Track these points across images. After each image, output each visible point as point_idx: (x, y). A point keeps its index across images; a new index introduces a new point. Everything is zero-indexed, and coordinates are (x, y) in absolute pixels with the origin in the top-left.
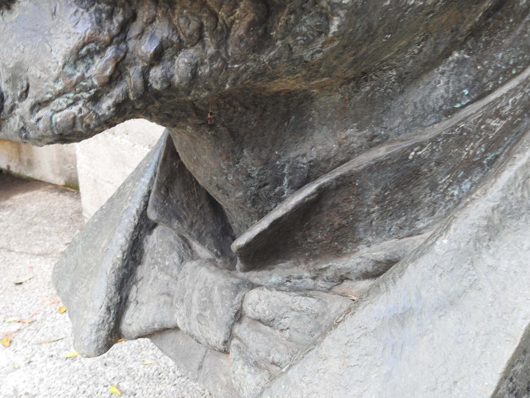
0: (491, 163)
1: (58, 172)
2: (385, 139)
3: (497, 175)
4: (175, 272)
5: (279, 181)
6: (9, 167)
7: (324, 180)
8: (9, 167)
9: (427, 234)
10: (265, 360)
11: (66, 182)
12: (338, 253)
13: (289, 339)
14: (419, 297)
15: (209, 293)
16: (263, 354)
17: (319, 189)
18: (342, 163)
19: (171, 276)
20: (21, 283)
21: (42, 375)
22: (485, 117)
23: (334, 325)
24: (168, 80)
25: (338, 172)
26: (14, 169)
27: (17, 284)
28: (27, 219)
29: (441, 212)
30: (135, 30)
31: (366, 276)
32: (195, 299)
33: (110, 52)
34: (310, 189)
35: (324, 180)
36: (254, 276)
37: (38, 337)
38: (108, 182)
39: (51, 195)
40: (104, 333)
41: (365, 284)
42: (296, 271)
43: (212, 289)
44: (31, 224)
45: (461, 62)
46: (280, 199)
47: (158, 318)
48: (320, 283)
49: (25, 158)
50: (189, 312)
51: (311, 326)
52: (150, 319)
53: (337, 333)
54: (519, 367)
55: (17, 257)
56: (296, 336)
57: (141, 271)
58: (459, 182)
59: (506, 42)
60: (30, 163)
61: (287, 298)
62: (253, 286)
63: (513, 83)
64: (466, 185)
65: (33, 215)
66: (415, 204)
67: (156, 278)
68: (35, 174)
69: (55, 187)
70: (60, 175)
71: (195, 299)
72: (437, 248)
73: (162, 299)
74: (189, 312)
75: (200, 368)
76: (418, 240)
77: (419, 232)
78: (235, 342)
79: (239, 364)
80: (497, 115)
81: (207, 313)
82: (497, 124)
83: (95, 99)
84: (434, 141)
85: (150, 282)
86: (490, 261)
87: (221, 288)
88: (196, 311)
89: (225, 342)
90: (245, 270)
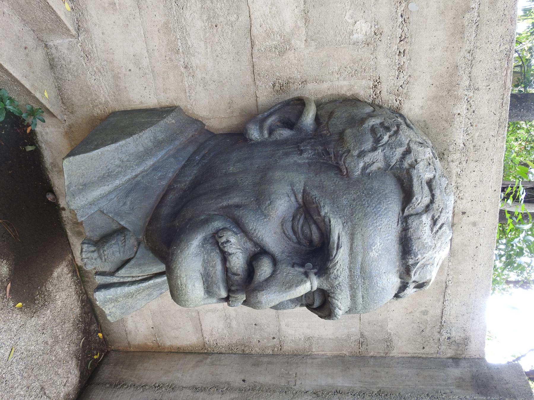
6: (64, 209)
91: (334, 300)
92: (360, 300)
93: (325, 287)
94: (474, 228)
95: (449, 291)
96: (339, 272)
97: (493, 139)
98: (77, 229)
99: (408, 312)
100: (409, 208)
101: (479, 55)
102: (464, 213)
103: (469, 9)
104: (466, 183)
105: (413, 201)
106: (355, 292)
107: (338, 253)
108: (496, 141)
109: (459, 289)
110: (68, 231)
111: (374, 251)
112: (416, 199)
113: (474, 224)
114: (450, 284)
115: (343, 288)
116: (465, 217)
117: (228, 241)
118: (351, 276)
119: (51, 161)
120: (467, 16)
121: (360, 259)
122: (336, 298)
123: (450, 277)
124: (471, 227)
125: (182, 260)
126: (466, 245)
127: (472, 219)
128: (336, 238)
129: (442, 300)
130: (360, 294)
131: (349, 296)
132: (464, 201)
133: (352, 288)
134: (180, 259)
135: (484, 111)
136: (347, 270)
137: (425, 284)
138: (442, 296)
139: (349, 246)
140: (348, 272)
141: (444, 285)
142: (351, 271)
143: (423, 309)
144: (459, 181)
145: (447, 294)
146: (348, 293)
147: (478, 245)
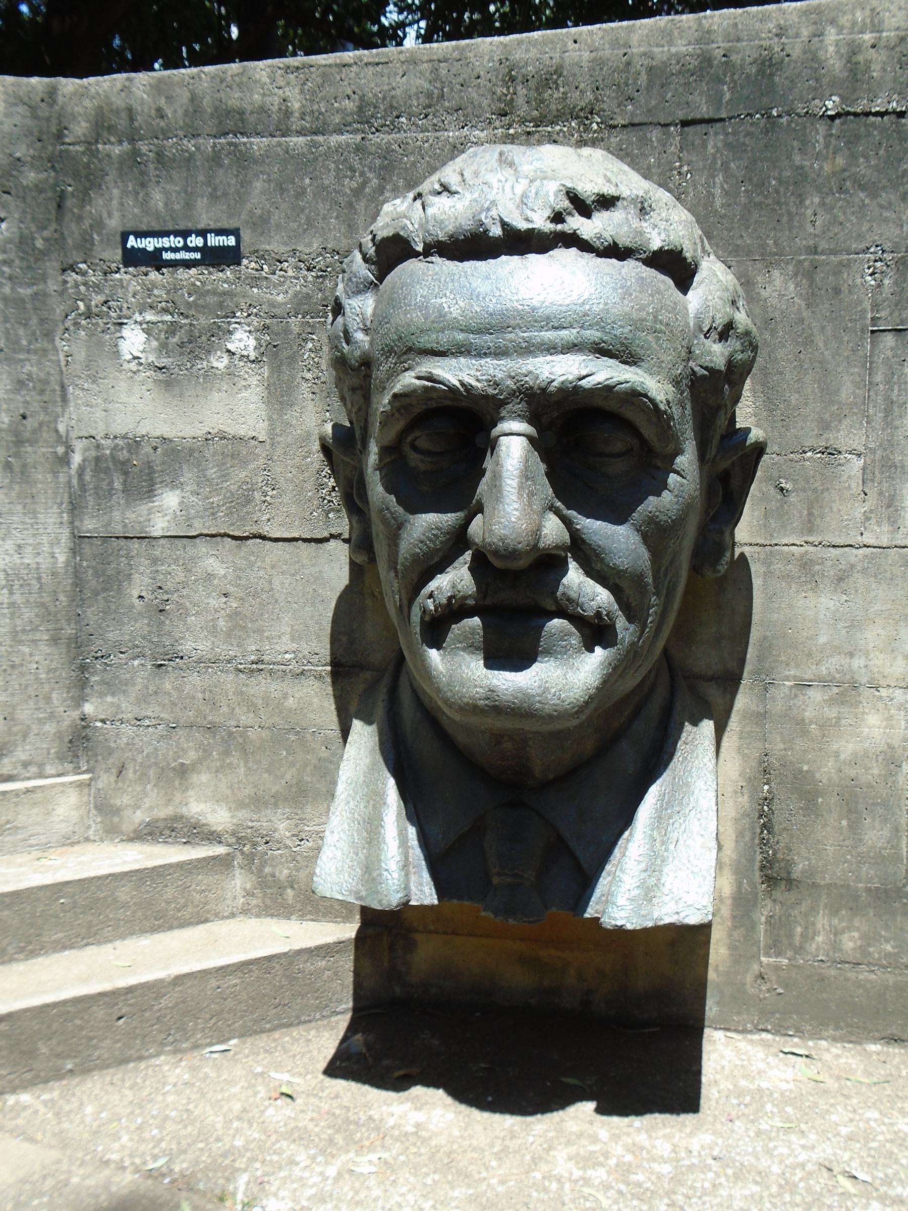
91: (551, 389)
96: (484, 378)
100: (415, 242)
105: (406, 236)
107: (441, 379)
108: (461, 62)
111: (452, 309)
112: (403, 228)
115: (524, 371)
117: (431, 596)
118: (500, 353)
121: (460, 337)
122: (543, 385)
125: (451, 691)
128: (418, 382)
130: (548, 335)
131: (549, 358)
133: (529, 349)
134: (449, 694)
136: (483, 362)
137: (571, 195)
139: (437, 358)
140: (488, 360)
142: (485, 354)
146: (540, 360)
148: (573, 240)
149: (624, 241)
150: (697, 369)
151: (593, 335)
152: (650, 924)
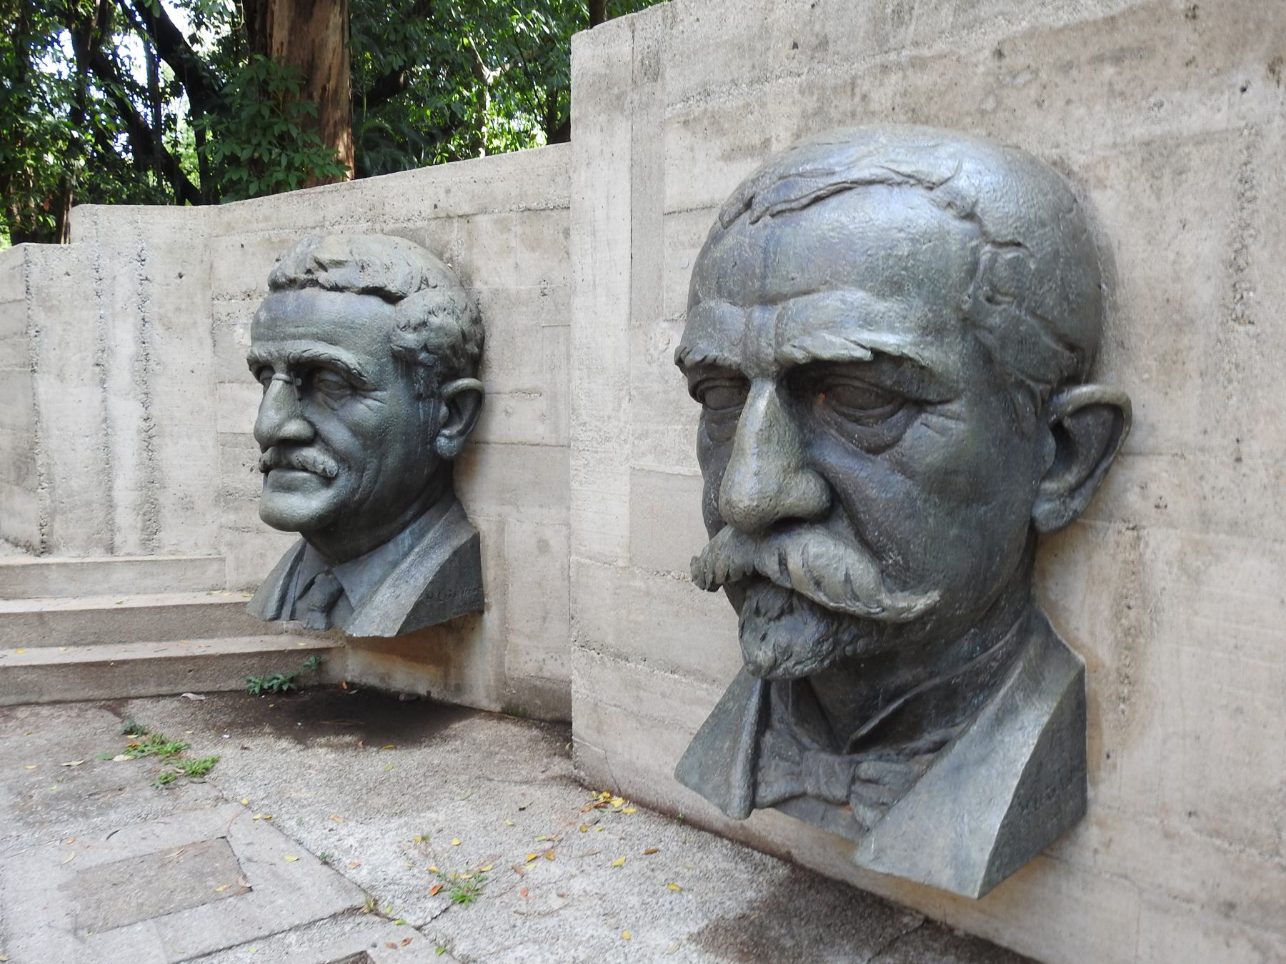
0: (993, 685)
1: (494, 696)
2: (938, 674)
3: (998, 691)
4: (798, 758)
5: (877, 698)
6: (429, 693)
7: (908, 696)
8: (429, 693)
9: (963, 726)
10: (877, 803)
11: (503, 708)
12: (911, 739)
13: (890, 789)
14: (965, 758)
15: (832, 767)
16: (875, 799)
17: (906, 702)
18: (915, 686)
19: (793, 762)
20: (524, 809)
21: (601, 880)
22: (988, 662)
23: (919, 777)
24: (855, 650)
25: (915, 691)
26: (435, 695)
27: (521, 809)
28: (484, 748)
29: (968, 712)
30: (841, 630)
31: (929, 751)
32: (821, 772)
33: (831, 640)
34: (900, 701)
35: (908, 696)
36: (857, 757)
37: (575, 853)
38: (615, 705)
39: (491, 723)
40: (748, 803)
41: (930, 756)
42: (885, 752)
43: (834, 765)
44: (491, 754)
45: (975, 634)
46: (877, 709)
47: (788, 789)
48: (901, 757)
49: (453, 682)
50: (818, 781)
51: (903, 780)
52: (783, 791)
53: (924, 779)
54: (1022, 791)
55: (501, 785)
56: (894, 788)
57: (762, 763)
58: (977, 696)
59: (996, 622)
60: (459, 689)
61: (887, 765)
62: (859, 763)
63: (1001, 643)
64: (981, 698)
65: (487, 744)
66: (954, 709)
67: (777, 766)
68: (465, 700)
69: (490, 714)
70: (496, 700)
71: (821, 772)
72: (971, 731)
73: (788, 777)
74: (818, 781)
75: (822, 819)
76: (958, 729)
77: (957, 725)
78: (852, 796)
79: (861, 807)
80: (994, 659)
81: (833, 779)
82: (995, 664)
83: (822, 661)
84: (964, 674)
85: (773, 768)
86: (1000, 738)
87: (840, 764)
88: (823, 780)
89: (847, 796)
90: (849, 753)
92: (301, 330)
93: (283, 366)
94: (453, 190)
95: (534, 205)
97: (365, 192)
98: (453, 688)
99: (565, 255)
101: (300, 223)
102: (436, 207)
103: (270, 239)
104: (404, 212)
106: (289, 335)
109: (530, 193)
110: (455, 701)
113: (448, 191)
114: (523, 205)
116: (440, 205)
119: (378, 680)
120: (273, 239)
123: (514, 207)
124: (451, 195)
126: (473, 196)
127: (442, 195)
129: (548, 212)
130: (293, 330)
132: (422, 210)
135: (341, 207)
138: (542, 213)
141: (526, 213)
143: (561, 236)
144: (402, 219)
145: (537, 207)
147: (472, 181)
148: (315, 283)
149: (341, 284)
150: (395, 347)
151: (315, 330)
152: (366, 635)
